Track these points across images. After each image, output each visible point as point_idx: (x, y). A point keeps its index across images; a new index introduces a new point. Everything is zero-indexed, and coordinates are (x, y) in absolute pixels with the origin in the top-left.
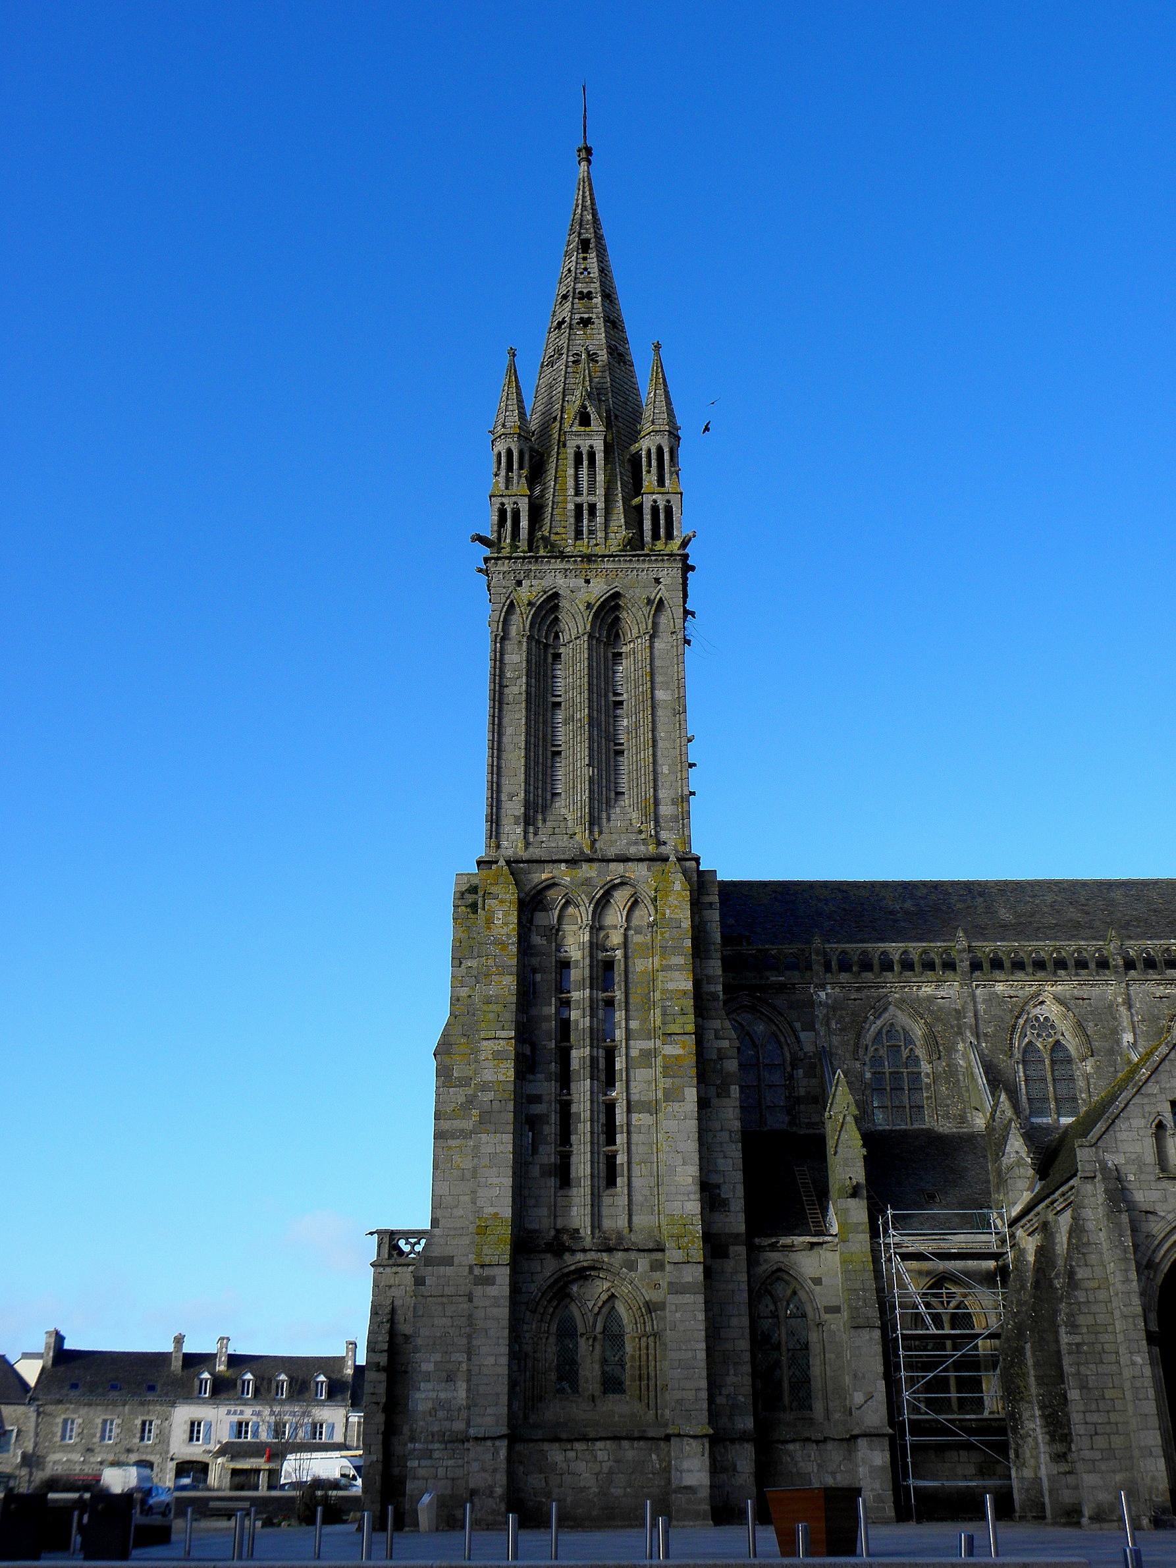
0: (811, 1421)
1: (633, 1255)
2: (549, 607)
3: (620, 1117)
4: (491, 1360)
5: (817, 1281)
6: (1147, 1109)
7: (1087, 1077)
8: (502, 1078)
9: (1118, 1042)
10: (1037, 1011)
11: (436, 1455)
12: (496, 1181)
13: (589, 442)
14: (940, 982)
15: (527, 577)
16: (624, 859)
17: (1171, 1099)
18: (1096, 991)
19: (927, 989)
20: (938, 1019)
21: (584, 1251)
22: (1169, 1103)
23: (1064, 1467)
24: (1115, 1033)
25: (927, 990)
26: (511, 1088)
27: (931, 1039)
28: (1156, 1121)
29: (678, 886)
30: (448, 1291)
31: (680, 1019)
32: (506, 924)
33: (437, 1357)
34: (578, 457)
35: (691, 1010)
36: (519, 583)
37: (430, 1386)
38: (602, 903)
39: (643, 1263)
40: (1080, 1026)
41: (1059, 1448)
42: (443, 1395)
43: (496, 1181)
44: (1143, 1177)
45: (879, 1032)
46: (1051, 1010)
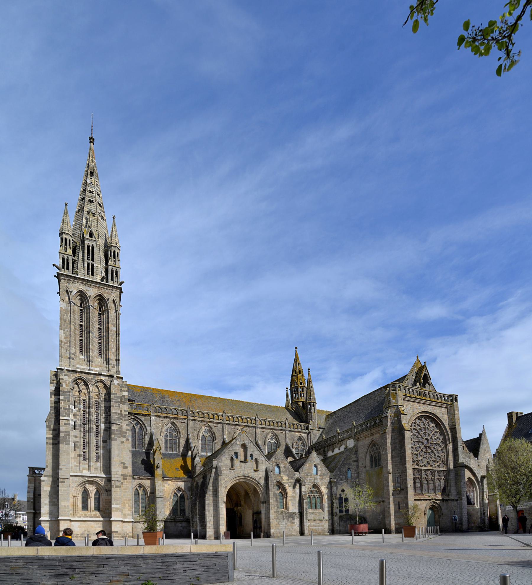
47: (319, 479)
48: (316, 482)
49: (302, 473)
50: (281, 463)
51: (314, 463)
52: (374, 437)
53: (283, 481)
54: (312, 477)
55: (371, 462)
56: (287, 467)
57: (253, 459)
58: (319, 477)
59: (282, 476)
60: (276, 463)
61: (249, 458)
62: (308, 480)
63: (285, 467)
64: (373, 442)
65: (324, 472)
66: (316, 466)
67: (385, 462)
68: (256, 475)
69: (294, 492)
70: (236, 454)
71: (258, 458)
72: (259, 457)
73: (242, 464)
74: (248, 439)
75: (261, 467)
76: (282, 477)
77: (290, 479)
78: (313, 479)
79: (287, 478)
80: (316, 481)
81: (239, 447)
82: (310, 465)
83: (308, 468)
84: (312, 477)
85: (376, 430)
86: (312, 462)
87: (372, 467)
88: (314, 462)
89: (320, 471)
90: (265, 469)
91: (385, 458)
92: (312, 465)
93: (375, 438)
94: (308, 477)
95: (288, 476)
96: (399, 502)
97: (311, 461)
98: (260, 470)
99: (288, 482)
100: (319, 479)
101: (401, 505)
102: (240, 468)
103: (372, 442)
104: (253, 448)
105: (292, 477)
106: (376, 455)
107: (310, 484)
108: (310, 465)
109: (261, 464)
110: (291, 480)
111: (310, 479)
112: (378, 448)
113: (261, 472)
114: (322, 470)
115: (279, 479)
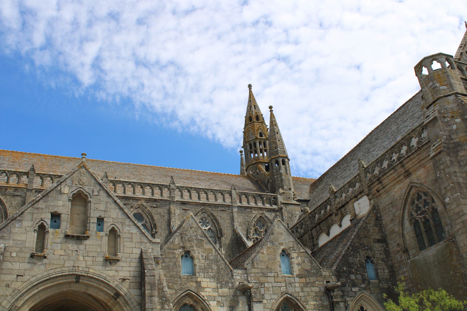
6: (35, 216)
17: (52, 211)
19: (10, 191)
22: (50, 214)
28: (40, 223)
44: (22, 255)
47: (297, 285)
48: (290, 292)
49: (254, 270)
50: (195, 248)
51: (282, 247)
52: (414, 178)
53: (203, 294)
54: (279, 279)
56: (212, 258)
57: (105, 228)
58: (297, 280)
59: (199, 280)
60: (184, 248)
61: (93, 227)
62: (268, 289)
63: (206, 258)
64: (413, 191)
65: (308, 266)
66: (285, 254)
67: (459, 221)
68: (111, 273)
71: (119, 226)
72: (123, 224)
73: (72, 246)
74: (93, 181)
75: (127, 250)
76: (199, 283)
77: (221, 287)
78: (283, 284)
79: (214, 285)
80: (291, 290)
81: (67, 199)
82: (272, 250)
83: (266, 258)
84: (279, 279)
85: (414, 160)
86: (277, 243)
88: (281, 244)
89: (298, 264)
90: (138, 256)
91: (456, 210)
92: (275, 251)
93: (416, 181)
94: (270, 279)
95: (218, 278)
97: (272, 242)
98: (124, 259)
99: (215, 294)
100: (297, 285)
102: (62, 252)
103: (410, 190)
104: (107, 203)
105: (227, 282)
107: (275, 297)
108: (272, 250)
109: (126, 244)
110: (225, 290)
111: (275, 284)
113: (128, 264)
114: (304, 262)
115: (193, 289)
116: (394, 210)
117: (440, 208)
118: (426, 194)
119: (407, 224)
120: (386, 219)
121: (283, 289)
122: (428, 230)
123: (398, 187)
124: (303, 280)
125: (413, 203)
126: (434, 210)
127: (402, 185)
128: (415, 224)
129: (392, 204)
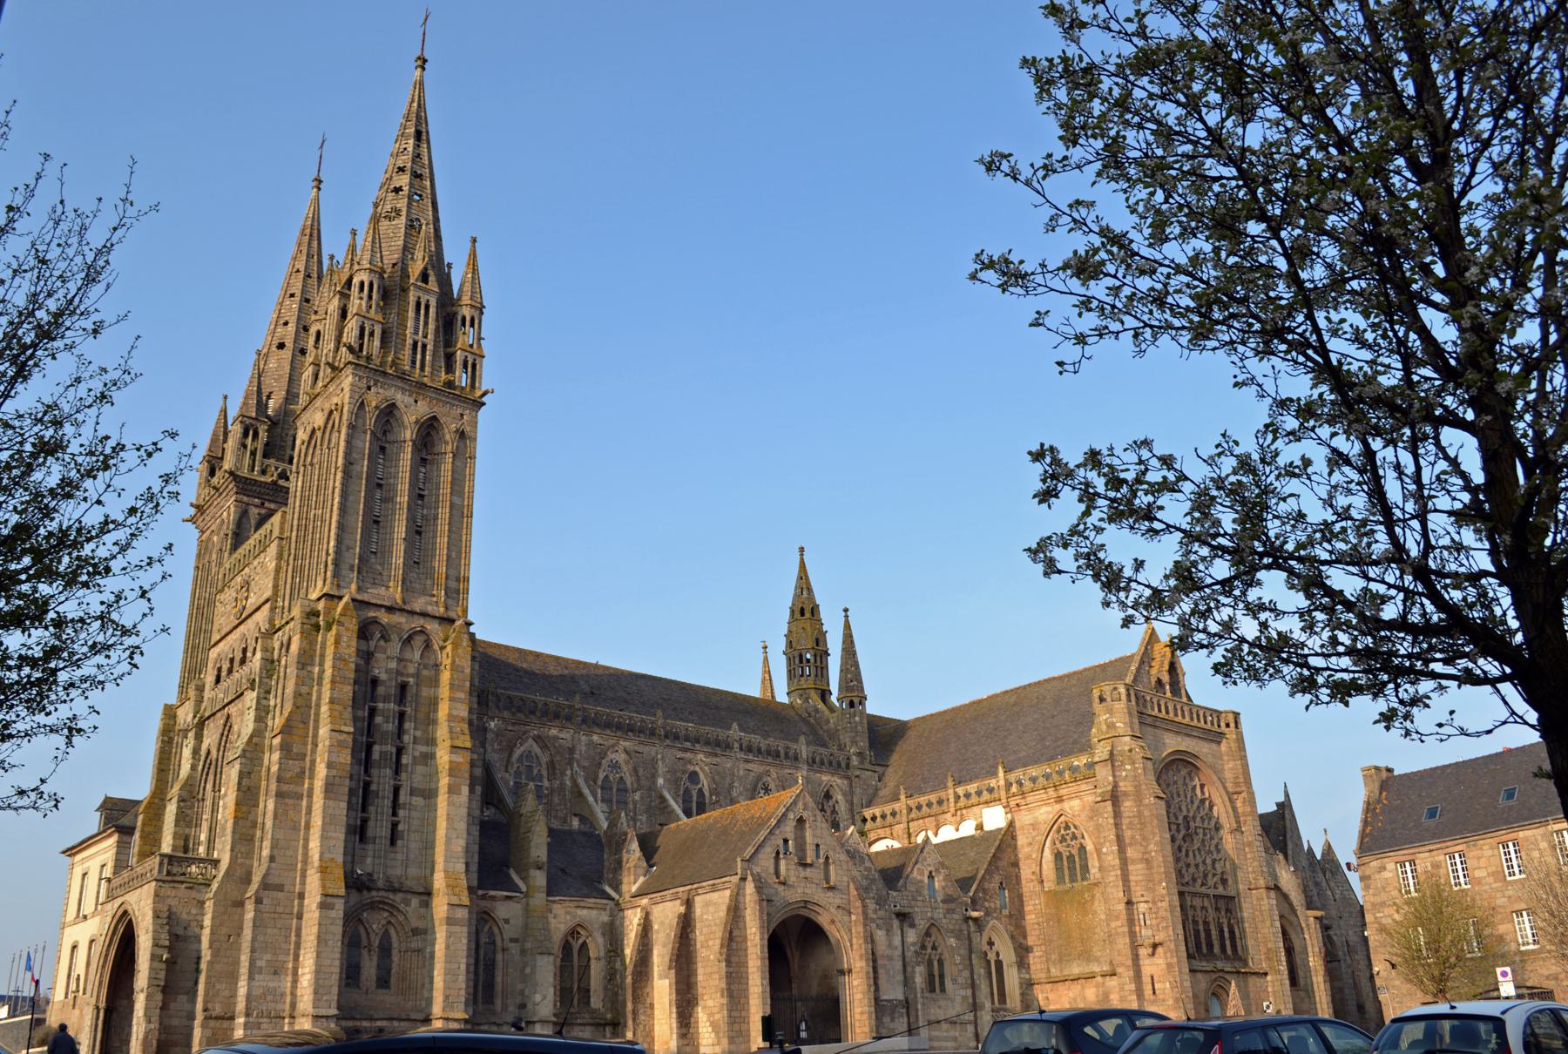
0: (494, 1013)
1: (409, 896)
2: (389, 413)
3: (402, 798)
4: (329, 962)
5: (507, 921)
7: (635, 803)
8: (343, 761)
9: (655, 783)
10: (613, 756)
11: (263, 1026)
12: (334, 835)
13: (426, 297)
14: (562, 728)
15: (375, 384)
16: (424, 615)
18: (646, 749)
20: (558, 752)
21: (379, 890)
23: (686, 1042)
24: (654, 777)
25: (554, 732)
26: (348, 768)
27: (551, 766)
29: (465, 644)
30: (280, 909)
31: (462, 737)
32: (349, 646)
33: (268, 957)
34: (418, 304)
35: (467, 732)
36: (369, 388)
37: (261, 977)
38: (408, 641)
39: (415, 902)
40: (635, 770)
41: (684, 1031)
42: (271, 985)
43: (334, 835)
45: (522, 755)
46: (621, 757)
52: (1066, 805)
55: (1059, 869)
64: (1062, 819)
69: (890, 945)
70: (786, 841)
87: (1060, 879)
94: (920, 904)
96: (1152, 978)
101: (1157, 986)
106: (1073, 852)
112: (1079, 836)
116: (1034, 834)
117: (1090, 847)
118: (1075, 827)
119: (1048, 853)
120: (1022, 840)
121: (929, 915)
122: (1072, 869)
123: (1045, 809)
124: (946, 906)
125: (1059, 831)
126: (1082, 848)
127: (1048, 809)
128: (1058, 856)
129: (1034, 826)
